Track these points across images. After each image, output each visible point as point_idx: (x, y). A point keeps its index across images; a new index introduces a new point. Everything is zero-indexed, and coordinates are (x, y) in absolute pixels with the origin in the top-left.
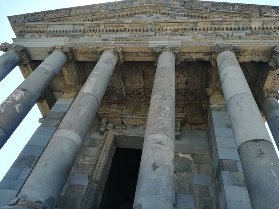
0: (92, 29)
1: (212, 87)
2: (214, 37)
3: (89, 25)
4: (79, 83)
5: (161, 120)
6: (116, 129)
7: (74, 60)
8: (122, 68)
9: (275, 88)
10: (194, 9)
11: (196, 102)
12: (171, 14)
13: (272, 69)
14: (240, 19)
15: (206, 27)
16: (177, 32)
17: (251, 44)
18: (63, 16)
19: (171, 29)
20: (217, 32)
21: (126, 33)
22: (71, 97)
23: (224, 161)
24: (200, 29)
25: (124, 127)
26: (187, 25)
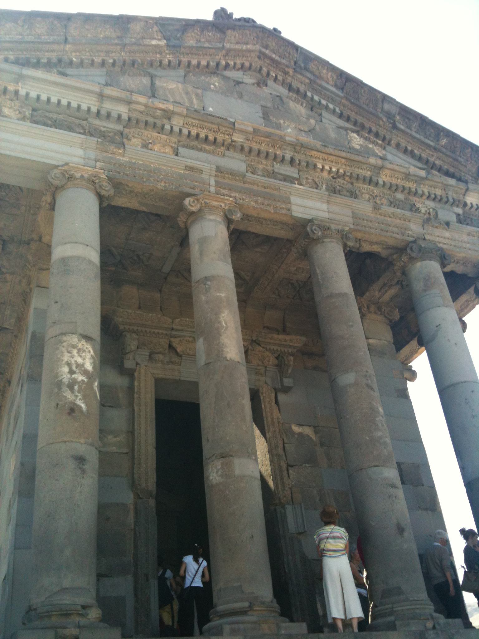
0: (151, 120)
3: (144, 107)
12: (312, 99)
15: (394, 181)
19: (330, 171)
20: (411, 198)
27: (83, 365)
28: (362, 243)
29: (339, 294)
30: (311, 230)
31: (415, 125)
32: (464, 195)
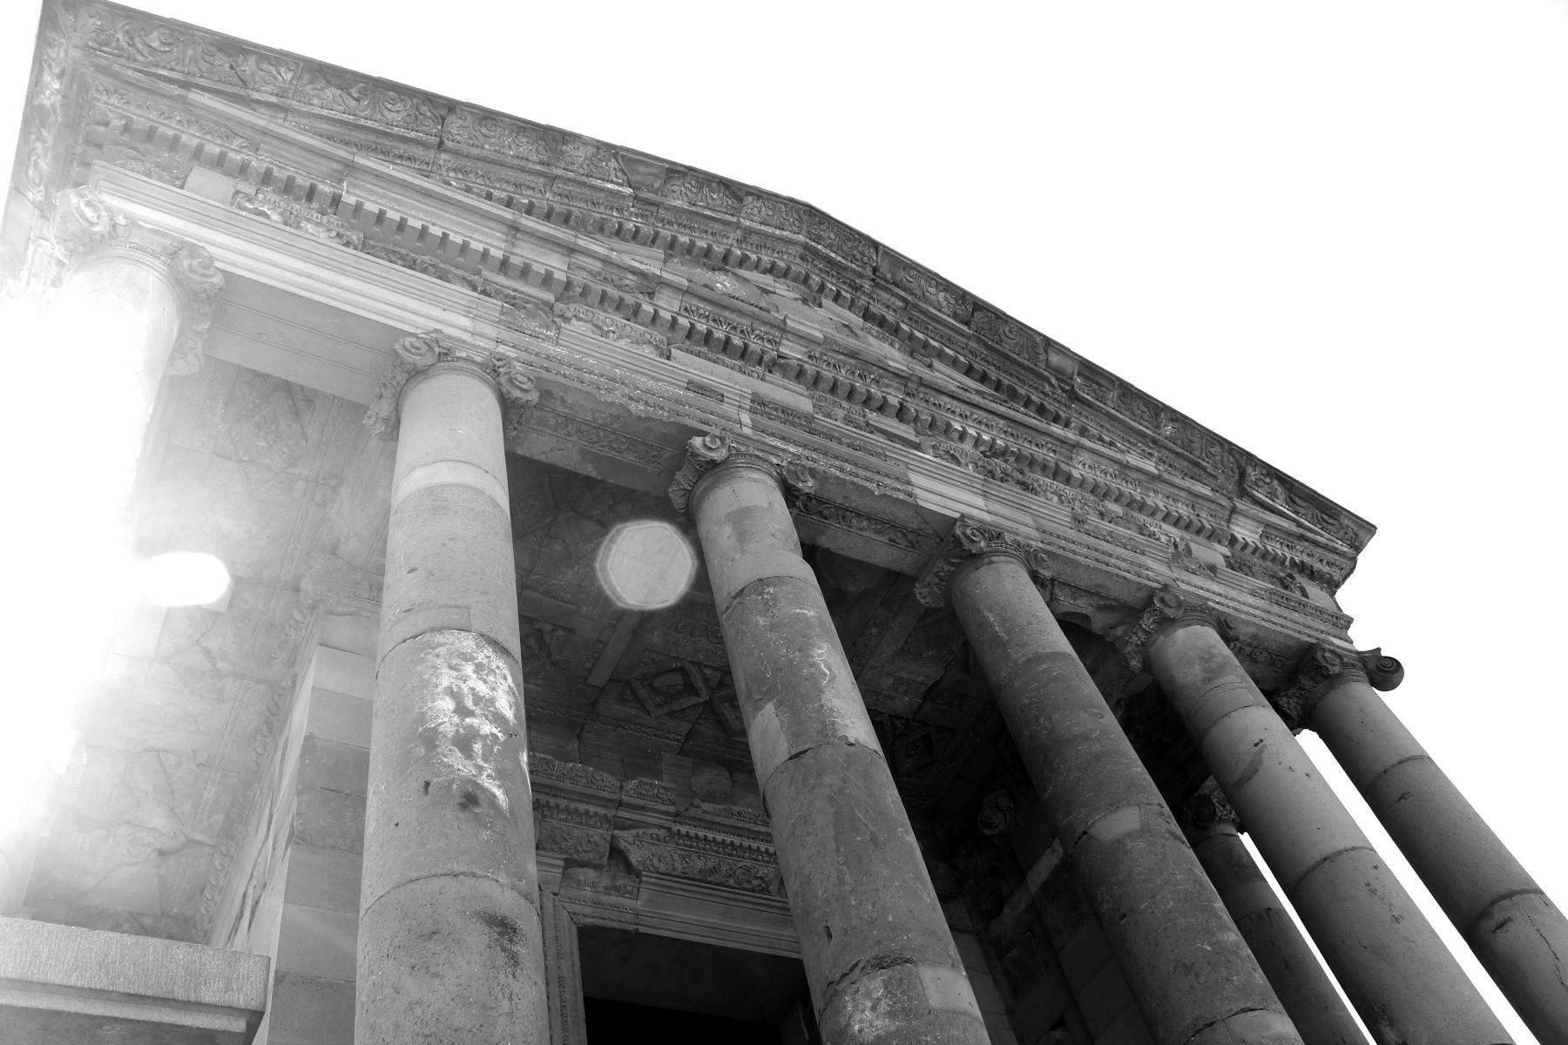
0: (613, 292)
10: (1013, 361)
15: (1101, 479)
19: (978, 442)
27: (492, 701)
30: (964, 534)
31: (1112, 395)
32: (1229, 521)
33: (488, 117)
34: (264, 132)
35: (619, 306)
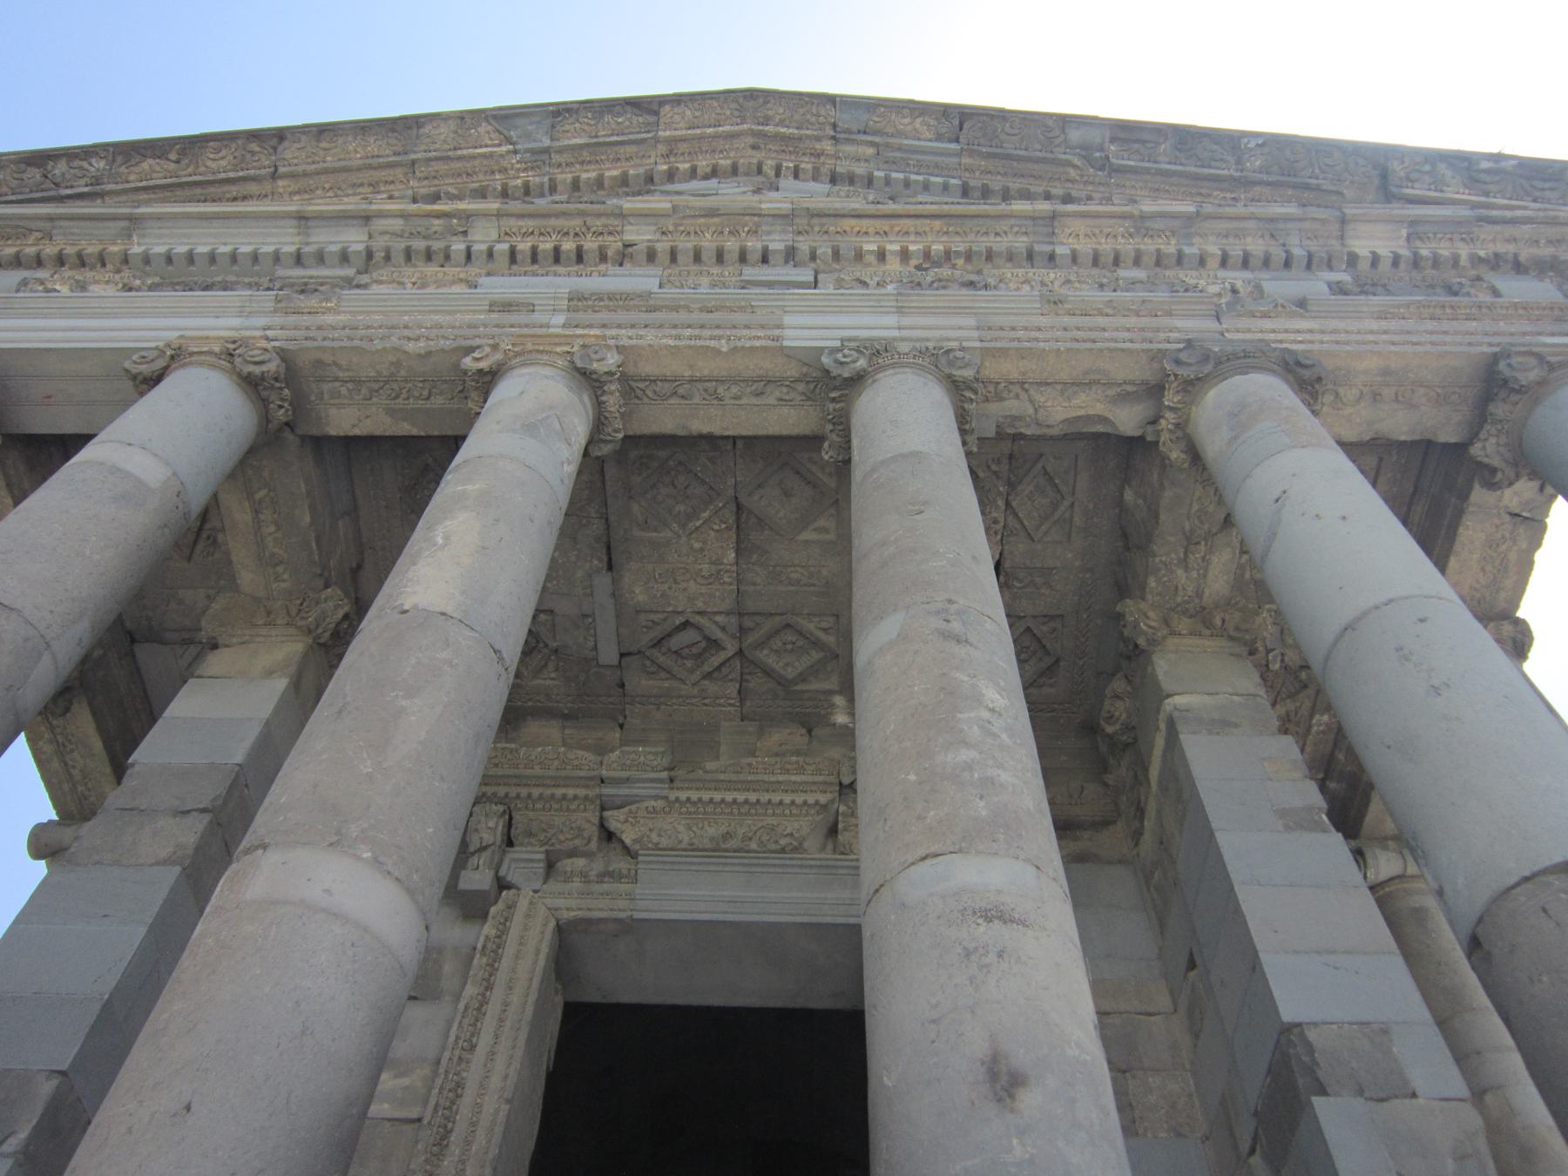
0: (419, 244)
1: (1160, 594)
2: (1161, 295)
3: (401, 222)
4: (320, 583)
5: (969, 766)
6: (568, 878)
7: (300, 432)
8: (603, 482)
9: (1503, 595)
10: (1019, 159)
11: (1053, 690)
13: (1490, 477)
14: (1292, 210)
15: (1106, 246)
16: (945, 272)
17: (1371, 337)
18: (232, 175)
19: (905, 255)
21: (638, 271)
22: (269, 673)
23: (1312, 1035)
24: (1075, 257)
25: (621, 864)
26: (997, 234)
28: (1040, 398)
29: (895, 458)
32: (1342, 237)
33: (323, 131)
34: (51, 218)
35: (429, 256)
